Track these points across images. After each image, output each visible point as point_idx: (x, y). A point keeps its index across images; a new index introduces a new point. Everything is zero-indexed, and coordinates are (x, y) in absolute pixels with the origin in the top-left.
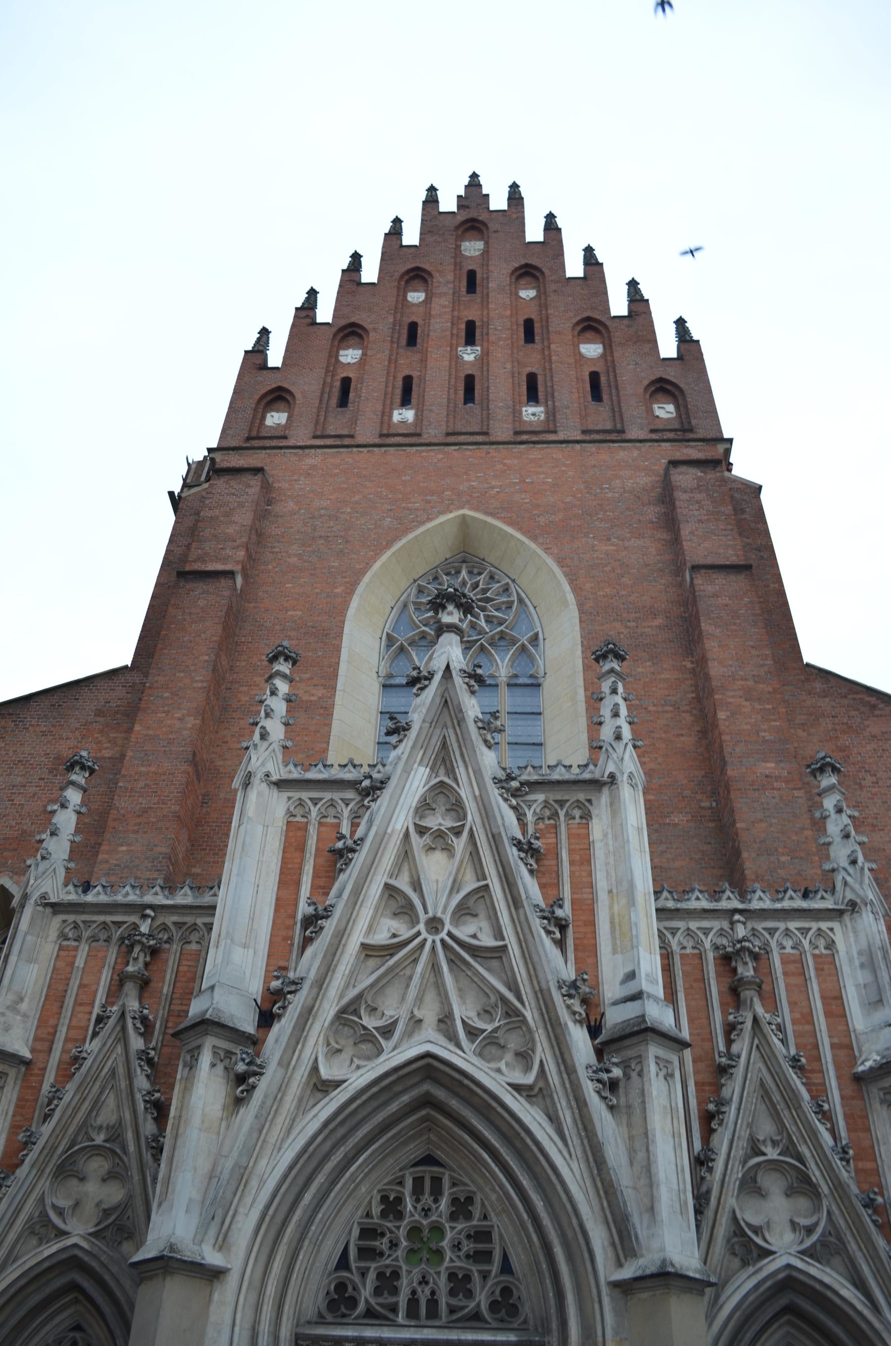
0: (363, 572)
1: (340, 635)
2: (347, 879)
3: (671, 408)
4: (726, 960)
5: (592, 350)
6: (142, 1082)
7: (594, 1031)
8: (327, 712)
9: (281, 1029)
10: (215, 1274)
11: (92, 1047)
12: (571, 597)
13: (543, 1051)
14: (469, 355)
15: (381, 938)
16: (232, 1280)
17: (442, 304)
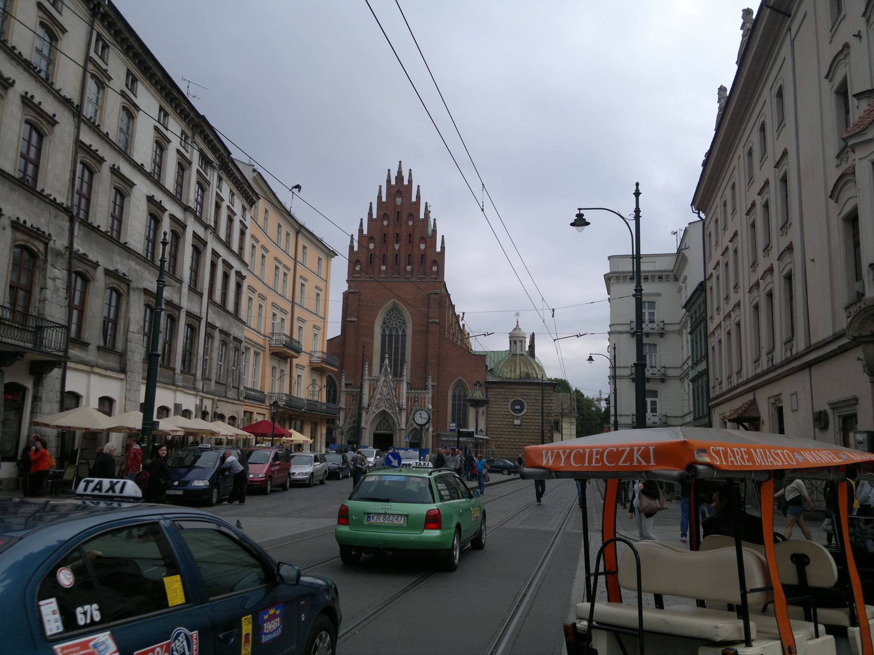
0: (376, 315)
1: (374, 329)
2: (376, 392)
3: (436, 267)
4: (415, 398)
5: (422, 246)
6: (357, 410)
7: (399, 407)
8: (373, 344)
9: (370, 408)
10: (366, 429)
11: (352, 407)
12: (411, 322)
13: (394, 409)
14: (397, 247)
15: (379, 398)
16: (368, 430)
17: (391, 228)
